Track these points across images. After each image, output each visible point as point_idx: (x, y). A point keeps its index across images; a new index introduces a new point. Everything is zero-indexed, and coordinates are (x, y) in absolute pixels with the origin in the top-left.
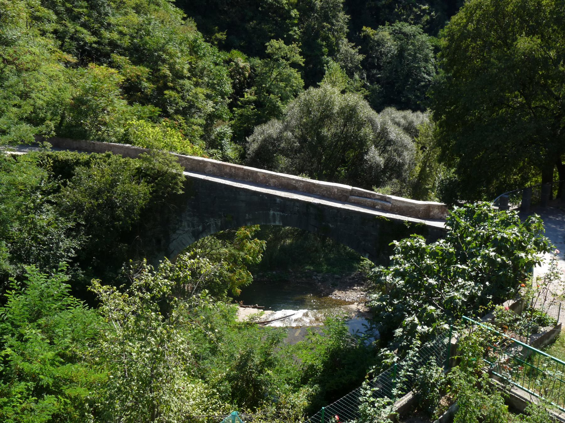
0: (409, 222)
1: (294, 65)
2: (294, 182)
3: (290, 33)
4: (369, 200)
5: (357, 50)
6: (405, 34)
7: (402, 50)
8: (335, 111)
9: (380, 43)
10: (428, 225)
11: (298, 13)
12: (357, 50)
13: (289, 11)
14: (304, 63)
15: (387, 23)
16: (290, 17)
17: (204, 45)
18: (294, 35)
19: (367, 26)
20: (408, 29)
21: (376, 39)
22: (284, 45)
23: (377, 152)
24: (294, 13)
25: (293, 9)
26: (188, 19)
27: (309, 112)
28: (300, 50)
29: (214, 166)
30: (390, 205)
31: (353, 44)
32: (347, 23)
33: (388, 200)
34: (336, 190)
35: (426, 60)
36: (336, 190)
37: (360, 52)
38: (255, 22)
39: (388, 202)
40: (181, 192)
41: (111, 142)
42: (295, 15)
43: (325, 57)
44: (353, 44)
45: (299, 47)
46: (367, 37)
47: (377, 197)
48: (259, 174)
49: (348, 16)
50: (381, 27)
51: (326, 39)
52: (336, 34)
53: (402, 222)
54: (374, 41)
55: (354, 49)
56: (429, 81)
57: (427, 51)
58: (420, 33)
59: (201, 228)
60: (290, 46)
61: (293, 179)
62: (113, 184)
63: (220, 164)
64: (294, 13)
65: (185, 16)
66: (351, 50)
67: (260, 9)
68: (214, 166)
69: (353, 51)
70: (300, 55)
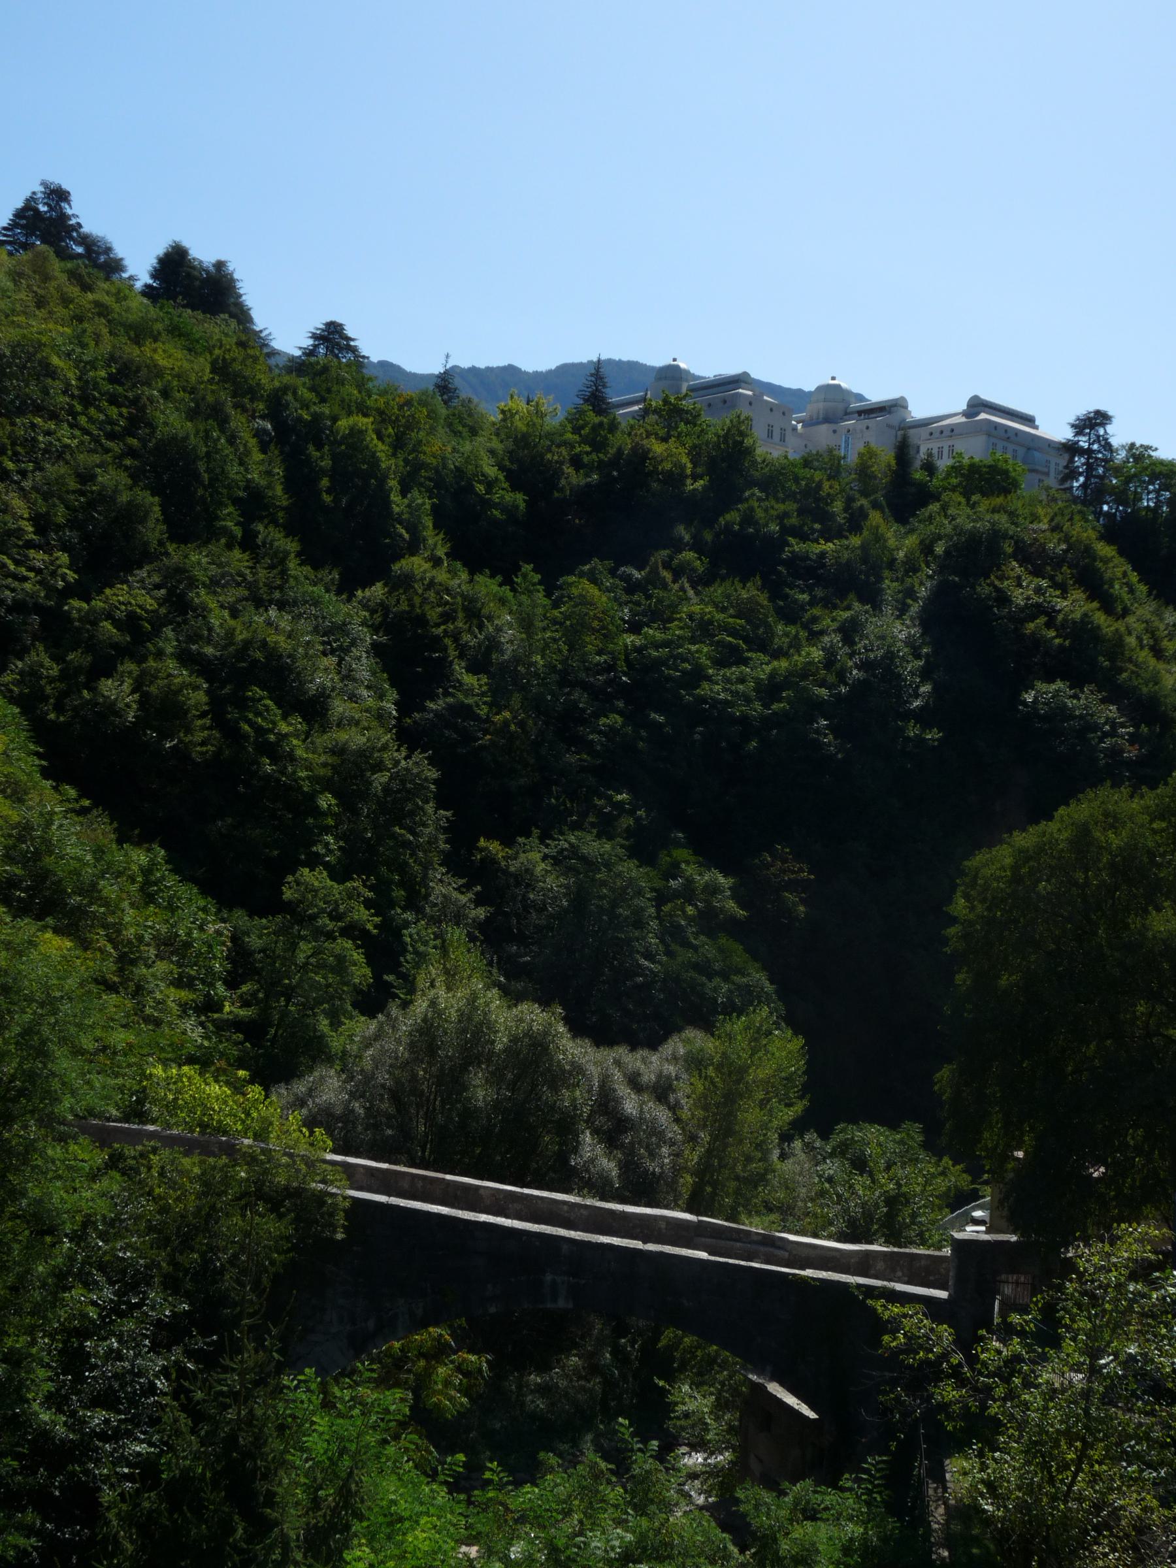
0: (859, 1286)
1: (353, 931)
2: (565, 1208)
3: (314, 849)
4: (738, 1244)
5: (470, 895)
6: (584, 859)
7: (579, 899)
8: (499, 1047)
9: (525, 879)
10: (900, 1292)
11: (333, 802)
12: (470, 895)
13: (312, 797)
14: (376, 927)
15: (536, 832)
16: (316, 812)
17: (171, 881)
18: (325, 856)
19: (488, 838)
20: (594, 846)
21: (512, 869)
22: (329, 883)
23: (599, 1149)
24: (326, 801)
25: (321, 793)
26: (95, 812)
27: (432, 1050)
28: (370, 895)
29: (372, 1175)
30: (786, 1255)
31: (461, 882)
32: (445, 830)
33: (779, 1243)
34: (663, 1225)
35: (639, 924)
36: (663, 1225)
37: (479, 901)
38: (229, 820)
39: (779, 1248)
40: (340, 1236)
41: (108, 1119)
42: (330, 805)
43: (399, 911)
44: (461, 882)
45: (371, 888)
46: (490, 861)
47: (755, 1238)
48: (482, 1192)
49: (448, 814)
50: (521, 840)
51: (402, 868)
52: (421, 854)
53: (846, 1285)
54: (505, 872)
55: (463, 893)
56: (655, 974)
57: (639, 902)
58: (621, 860)
59: (371, 1324)
60: (348, 884)
61: (564, 1203)
62: (209, 1216)
63: (387, 1170)
64: (326, 801)
65: (86, 803)
66: (455, 895)
67: (241, 789)
68: (372, 1175)
69: (463, 899)
70: (367, 908)
